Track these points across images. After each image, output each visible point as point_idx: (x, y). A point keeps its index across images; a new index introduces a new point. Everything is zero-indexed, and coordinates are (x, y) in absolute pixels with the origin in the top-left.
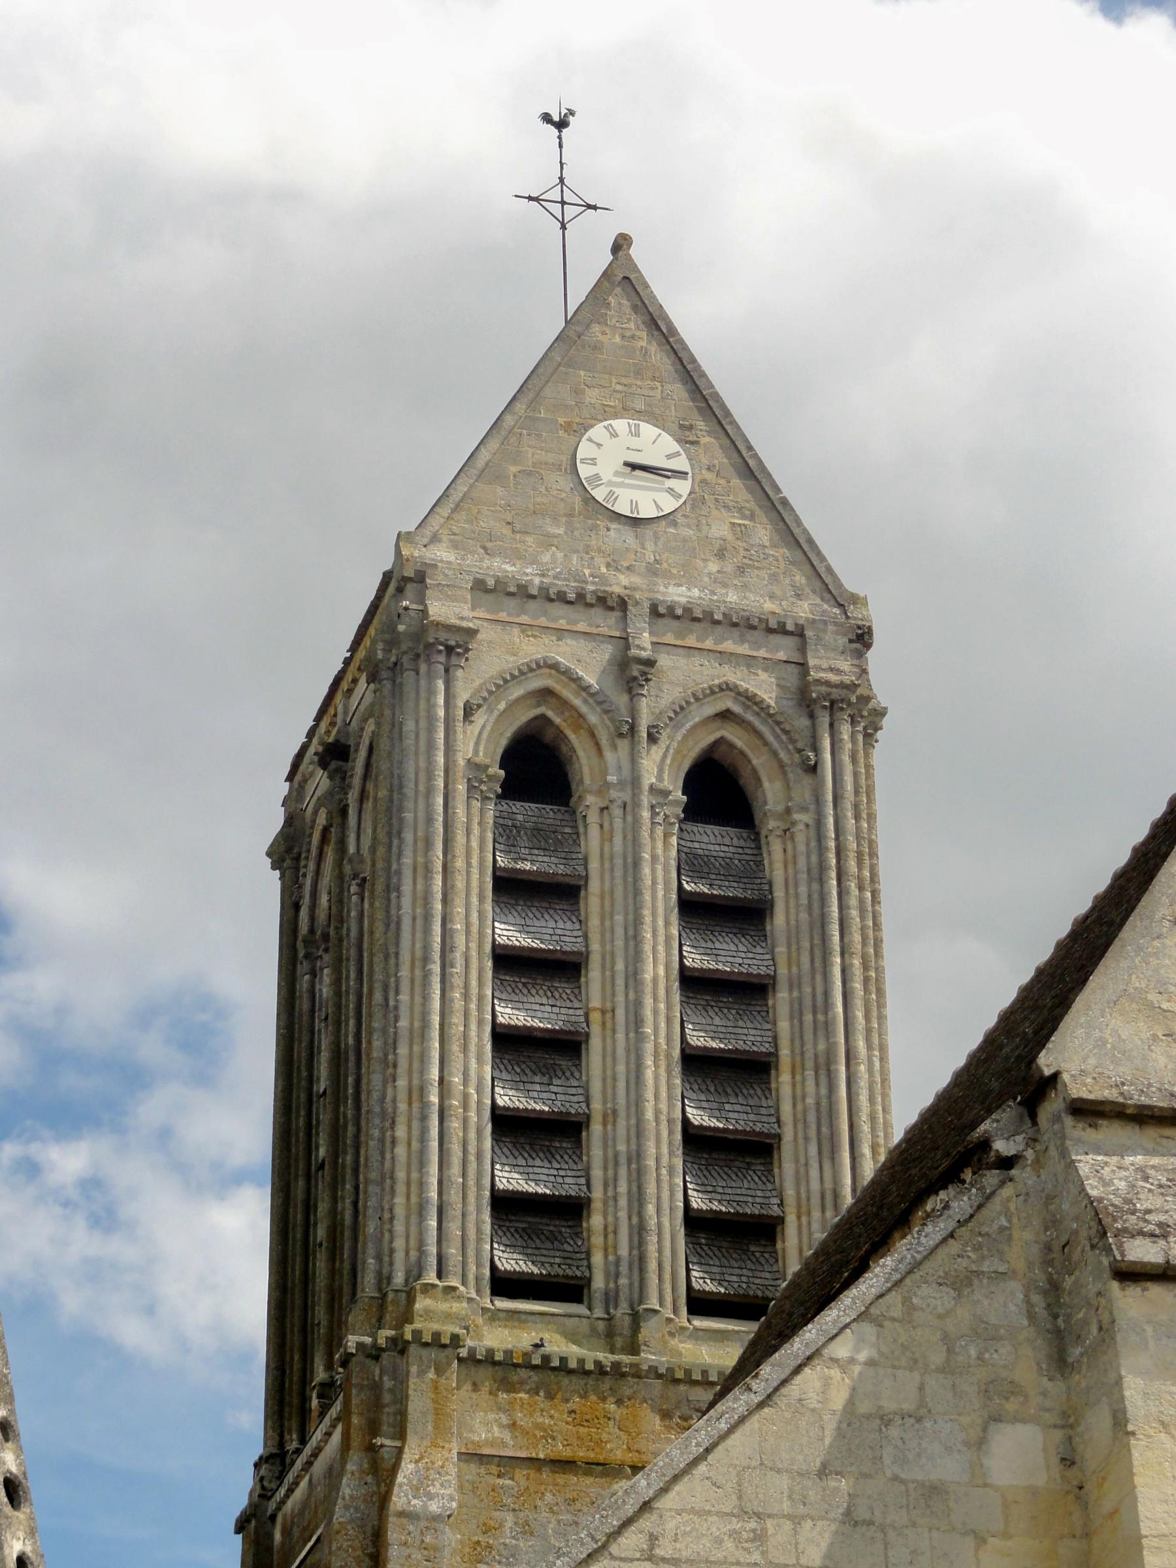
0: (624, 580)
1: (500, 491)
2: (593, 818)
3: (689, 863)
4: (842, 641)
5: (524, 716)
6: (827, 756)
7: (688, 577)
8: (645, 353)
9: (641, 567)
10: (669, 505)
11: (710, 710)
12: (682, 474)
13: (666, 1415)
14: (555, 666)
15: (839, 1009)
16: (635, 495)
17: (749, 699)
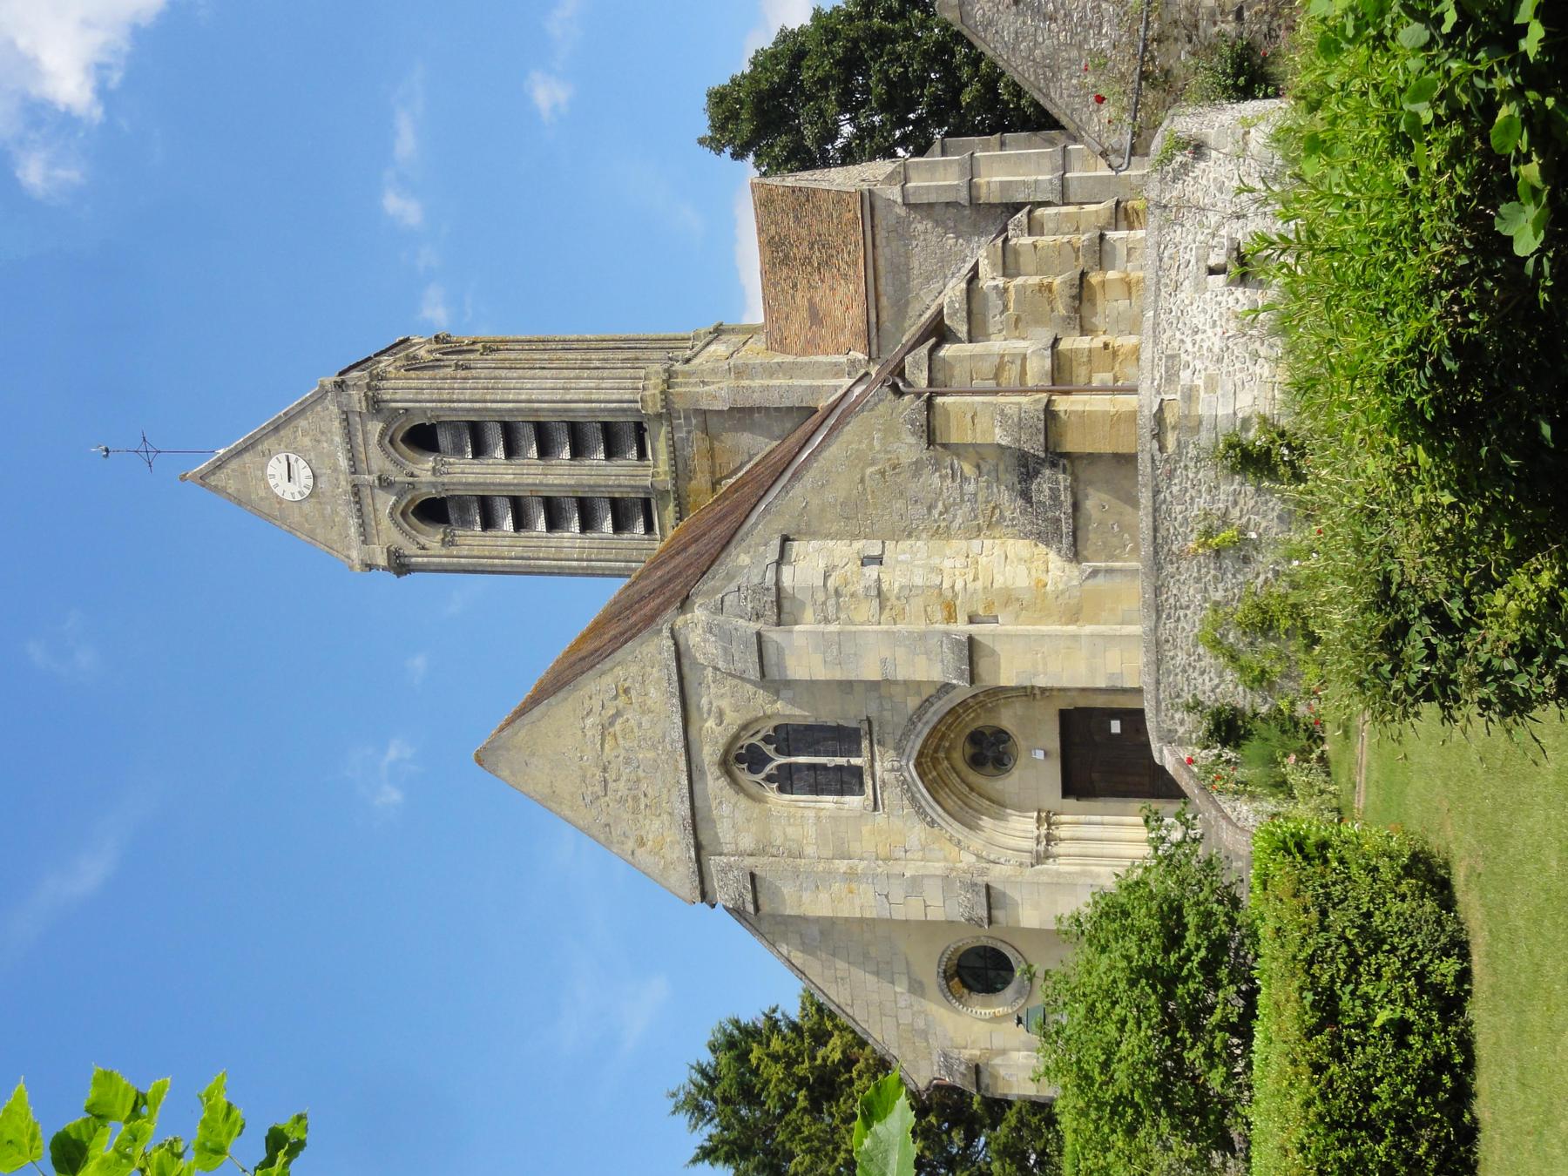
0: (343, 483)
1: (318, 531)
2: (450, 493)
3: (459, 451)
5: (413, 520)
6: (399, 405)
7: (332, 455)
8: (233, 470)
9: (335, 475)
10: (302, 463)
11: (392, 450)
12: (288, 458)
13: (691, 479)
14: (391, 513)
15: (510, 405)
17: (382, 435)
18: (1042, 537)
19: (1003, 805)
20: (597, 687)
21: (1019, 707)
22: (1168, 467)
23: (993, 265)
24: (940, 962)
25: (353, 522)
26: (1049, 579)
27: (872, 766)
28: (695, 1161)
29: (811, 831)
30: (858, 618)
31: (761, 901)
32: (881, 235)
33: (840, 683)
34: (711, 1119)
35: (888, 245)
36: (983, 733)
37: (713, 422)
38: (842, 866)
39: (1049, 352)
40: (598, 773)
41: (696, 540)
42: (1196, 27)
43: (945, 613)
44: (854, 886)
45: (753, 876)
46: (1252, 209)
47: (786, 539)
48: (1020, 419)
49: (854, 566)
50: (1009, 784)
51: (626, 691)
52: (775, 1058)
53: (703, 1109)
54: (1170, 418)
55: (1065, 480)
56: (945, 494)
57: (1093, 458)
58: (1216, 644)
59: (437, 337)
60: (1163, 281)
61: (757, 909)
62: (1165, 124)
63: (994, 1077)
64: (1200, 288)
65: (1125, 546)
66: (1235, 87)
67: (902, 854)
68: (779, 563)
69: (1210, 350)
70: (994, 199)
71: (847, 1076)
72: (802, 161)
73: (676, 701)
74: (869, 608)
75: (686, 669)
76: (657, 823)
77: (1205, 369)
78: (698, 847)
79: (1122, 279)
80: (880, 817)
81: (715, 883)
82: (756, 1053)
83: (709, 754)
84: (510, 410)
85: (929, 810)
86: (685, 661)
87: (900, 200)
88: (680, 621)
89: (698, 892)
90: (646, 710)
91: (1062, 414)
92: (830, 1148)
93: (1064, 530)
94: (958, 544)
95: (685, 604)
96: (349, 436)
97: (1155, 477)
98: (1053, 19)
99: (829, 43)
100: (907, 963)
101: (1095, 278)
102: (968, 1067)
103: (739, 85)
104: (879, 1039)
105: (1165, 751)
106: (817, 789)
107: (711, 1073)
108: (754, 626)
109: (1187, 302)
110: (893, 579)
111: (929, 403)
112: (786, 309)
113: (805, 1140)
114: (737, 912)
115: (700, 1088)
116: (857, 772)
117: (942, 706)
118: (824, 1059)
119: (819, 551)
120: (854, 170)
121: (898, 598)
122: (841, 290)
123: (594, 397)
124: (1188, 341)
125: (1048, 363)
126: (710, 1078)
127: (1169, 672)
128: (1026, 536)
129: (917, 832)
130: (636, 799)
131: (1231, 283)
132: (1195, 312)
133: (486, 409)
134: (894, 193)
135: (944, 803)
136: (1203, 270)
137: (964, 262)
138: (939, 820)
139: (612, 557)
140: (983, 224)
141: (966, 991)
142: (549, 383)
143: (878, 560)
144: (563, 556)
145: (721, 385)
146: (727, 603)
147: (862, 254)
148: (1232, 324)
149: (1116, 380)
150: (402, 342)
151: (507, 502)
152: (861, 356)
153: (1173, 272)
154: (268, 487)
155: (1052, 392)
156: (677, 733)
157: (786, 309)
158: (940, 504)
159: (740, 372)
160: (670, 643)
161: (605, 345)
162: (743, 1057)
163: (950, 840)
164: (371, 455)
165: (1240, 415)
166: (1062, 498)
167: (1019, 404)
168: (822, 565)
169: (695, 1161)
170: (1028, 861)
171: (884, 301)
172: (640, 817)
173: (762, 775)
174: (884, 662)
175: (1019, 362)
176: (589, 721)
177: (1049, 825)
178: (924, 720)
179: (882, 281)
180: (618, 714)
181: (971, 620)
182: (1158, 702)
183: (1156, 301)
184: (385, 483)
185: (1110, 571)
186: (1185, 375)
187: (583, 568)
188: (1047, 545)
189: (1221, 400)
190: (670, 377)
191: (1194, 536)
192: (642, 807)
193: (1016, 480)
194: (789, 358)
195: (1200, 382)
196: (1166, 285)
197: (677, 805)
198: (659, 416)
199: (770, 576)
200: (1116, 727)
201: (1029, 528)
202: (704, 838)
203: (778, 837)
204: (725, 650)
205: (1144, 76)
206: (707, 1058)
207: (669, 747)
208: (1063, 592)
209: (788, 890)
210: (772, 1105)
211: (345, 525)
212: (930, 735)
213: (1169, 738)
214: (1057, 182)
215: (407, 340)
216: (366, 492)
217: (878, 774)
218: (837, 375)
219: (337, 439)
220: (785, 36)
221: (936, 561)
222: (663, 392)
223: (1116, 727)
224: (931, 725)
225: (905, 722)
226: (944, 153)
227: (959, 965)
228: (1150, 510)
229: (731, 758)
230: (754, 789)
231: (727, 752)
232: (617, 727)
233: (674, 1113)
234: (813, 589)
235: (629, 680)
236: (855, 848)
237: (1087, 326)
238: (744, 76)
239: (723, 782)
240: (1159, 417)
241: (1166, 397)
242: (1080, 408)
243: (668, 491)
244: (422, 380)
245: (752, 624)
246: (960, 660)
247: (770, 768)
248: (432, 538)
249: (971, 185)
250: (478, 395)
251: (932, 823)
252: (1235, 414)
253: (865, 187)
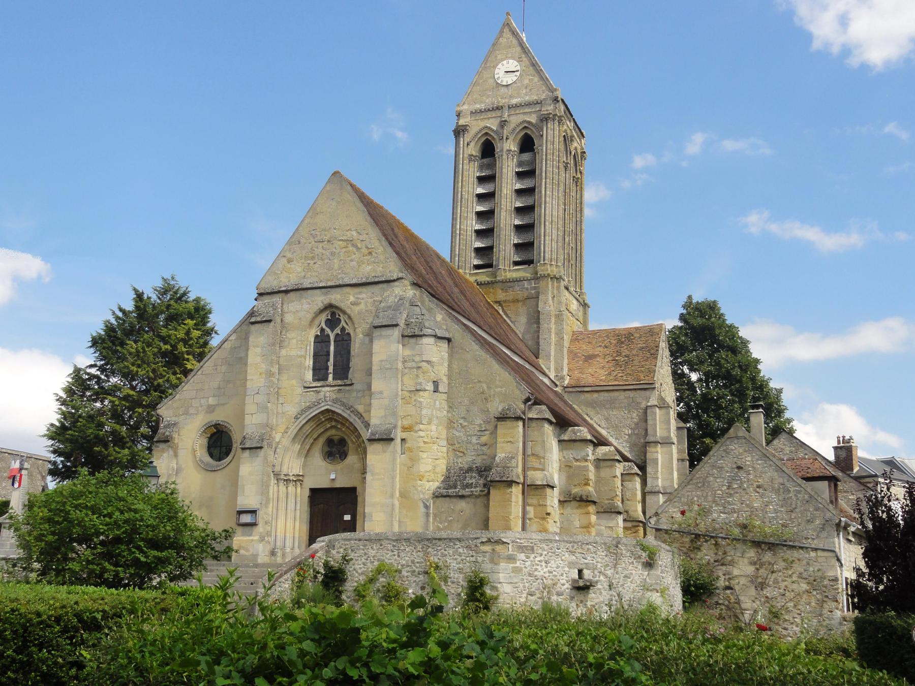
0: (504, 101)
2: (497, 159)
3: (520, 164)
4: (551, 102)
5: (484, 139)
6: (545, 132)
8: (511, 41)
10: (515, 79)
11: (521, 128)
12: (517, 71)
13: (502, 290)
14: (487, 127)
16: (507, 79)
17: (529, 122)
18: (447, 478)
19: (306, 456)
20: (373, 237)
21: (358, 465)
22: (473, 546)
23: (605, 454)
24: (224, 422)
25: (482, 106)
26: (424, 482)
27: (327, 386)
28: (135, 290)
29: (293, 353)
30: (405, 378)
31: (256, 325)
32: (631, 394)
33: (371, 369)
34: (159, 298)
36: (345, 446)
37: (533, 302)
38: (275, 369)
39: (545, 483)
40: (327, 238)
41: (462, 292)
42: (722, 565)
43: (406, 426)
44: (264, 376)
45: (270, 321)
46: (615, 594)
47: (449, 340)
48: (508, 467)
49: (433, 376)
50: (318, 460)
51: (370, 253)
52: (188, 333)
53: (165, 294)
54: (499, 548)
55: (476, 492)
56: (471, 426)
57: (487, 507)
58: (379, 571)
59: (584, 152)
60: (575, 545)
61: (253, 323)
62: (663, 545)
63: (163, 451)
64: (571, 565)
65: (441, 523)
66: (690, 585)
67: (281, 402)
68: (435, 336)
69: (536, 570)
70: (649, 455)
71: (178, 371)
72: (676, 352)
73: (364, 280)
74: (409, 383)
75: (381, 286)
76: (299, 270)
77: (525, 567)
78: (286, 292)
79: (590, 523)
80: (300, 390)
81: (267, 300)
82: (190, 322)
83: (335, 297)
84: (541, 192)
85: (304, 416)
86: (385, 285)
87: (649, 404)
88: (407, 282)
89: (263, 291)
90: (360, 264)
91: (510, 490)
92: (139, 362)
93: (450, 491)
94: (444, 433)
95: (415, 285)
96: (529, 104)
97: (467, 539)
98: (729, 487)
99: (740, 367)
100: (224, 404)
101: (592, 509)
102: (167, 436)
103: (720, 318)
104: (184, 389)
105: (323, 544)
106: (316, 355)
107: (184, 299)
108: (402, 323)
109: (563, 558)
110: (425, 398)
111: (518, 418)
112: (594, 342)
113: (143, 348)
114: (252, 314)
115: (176, 293)
116: (325, 378)
117: (358, 424)
118: (188, 360)
119: (442, 358)
120: (669, 380)
121: (415, 400)
122: (602, 372)
123: (547, 238)
124: (542, 558)
125: (539, 483)
126: (180, 297)
127: (365, 546)
128: (448, 470)
129: (292, 410)
130: (313, 258)
131: (574, 581)
133: (541, 179)
134: (653, 401)
135: (307, 425)
136: (581, 567)
137: (616, 439)
138: (298, 421)
139: (461, 247)
140: (636, 449)
141: (209, 435)
142: (555, 213)
143: (436, 390)
144: (462, 220)
145: (552, 308)
146: (415, 308)
147: (621, 383)
148: (550, 582)
149: (530, 519)
150: (582, 134)
151: (492, 190)
152: (566, 382)
153: (580, 551)
154: (503, 60)
155: (523, 484)
156: (347, 281)
157: (594, 342)
158: (466, 424)
159: (559, 317)
160: (395, 277)
161: (579, 244)
162: (191, 317)
163: (287, 428)
164: (519, 116)
165: (499, 586)
166: (467, 490)
167: (517, 467)
168: (434, 359)
169: (135, 290)
170: (275, 470)
171: (595, 395)
172: (303, 261)
173: (324, 327)
174: (381, 393)
175: (540, 467)
176: (354, 233)
177: (295, 481)
178: (352, 414)
179: (606, 394)
180: (358, 249)
181: (403, 440)
182: (349, 540)
183: (564, 541)
184: (503, 124)
185: (427, 515)
186: (522, 556)
187: (456, 231)
188: (443, 481)
189: (508, 575)
190: (557, 279)
191: (436, 560)
192: (308, 262)
193: (478, 465)
194: (566, 344)
195: (518, 564)
196: (573, 547)
197: (309, 281)
198: (537, 274)
199: (429, 331)
200: (347, 517)
201: (452, 471)
202: (292, 294)
203: (290, 335)
204: (390, 307)
205: (697, 536)
206: (192, 296)
207: (340, 276)
208: (417, 490)
209: (262, 340)
210: (164, 332)
211: (481, 102)
212: (344, 417)
213: (330, 546)
214: (657, 489)
215: (583, 137)
216: (498, 113)
217: (323, 389)
218: (556, 369)
219: (527, 98)
220: (745, 343)
221: (435, 421)
222: (549, 275)
223: (347, 517)
224: (348, 418)
225: (350, 404)
226: (679, 428)
227: (223, 431)
228: (451, 537)
229: (334, 310)
230: (317, 322)
231: (337, 307)
232: (351, 248)
233: (163, 278)
234: (421, 355)
235: (376, 255)
236: (284, 377)
237: (566, 504)
238: (724, 320)
239: (321, 306)
240: (499, 542)
241: (510, 546)
242: (514, 499)
243: (496, 277)
244: (558, 144)
245: (404, 321)
246: (381, 434)
247: (328, 330)
248: (474, 149)
249: (657, 442)
250: (550, 175)
251: (296, 418)
252: (500, 583)
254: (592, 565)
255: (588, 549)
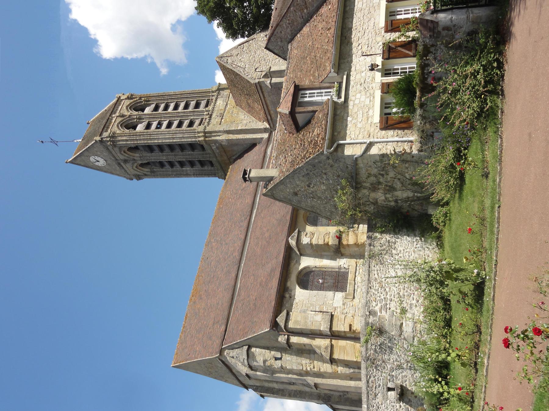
11: (125, 154)
32: (266, 94)
35: (269, 96)
49: (273, 361)
79: (355, 244)
132: (384, 408)
136: (385, 389)
143: (280, 359)
153: (374, 389)
196: (371, 394)
253: (257, 81)
254: (385, 381)
255: (372, 382)
